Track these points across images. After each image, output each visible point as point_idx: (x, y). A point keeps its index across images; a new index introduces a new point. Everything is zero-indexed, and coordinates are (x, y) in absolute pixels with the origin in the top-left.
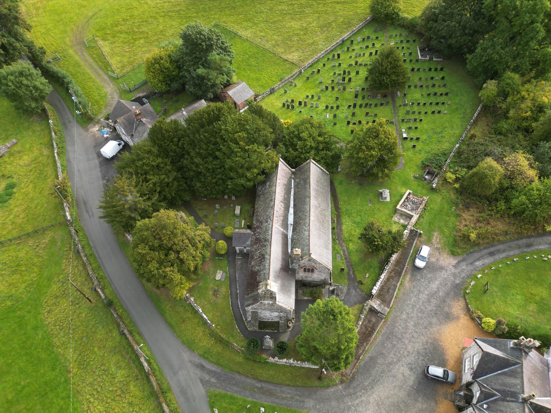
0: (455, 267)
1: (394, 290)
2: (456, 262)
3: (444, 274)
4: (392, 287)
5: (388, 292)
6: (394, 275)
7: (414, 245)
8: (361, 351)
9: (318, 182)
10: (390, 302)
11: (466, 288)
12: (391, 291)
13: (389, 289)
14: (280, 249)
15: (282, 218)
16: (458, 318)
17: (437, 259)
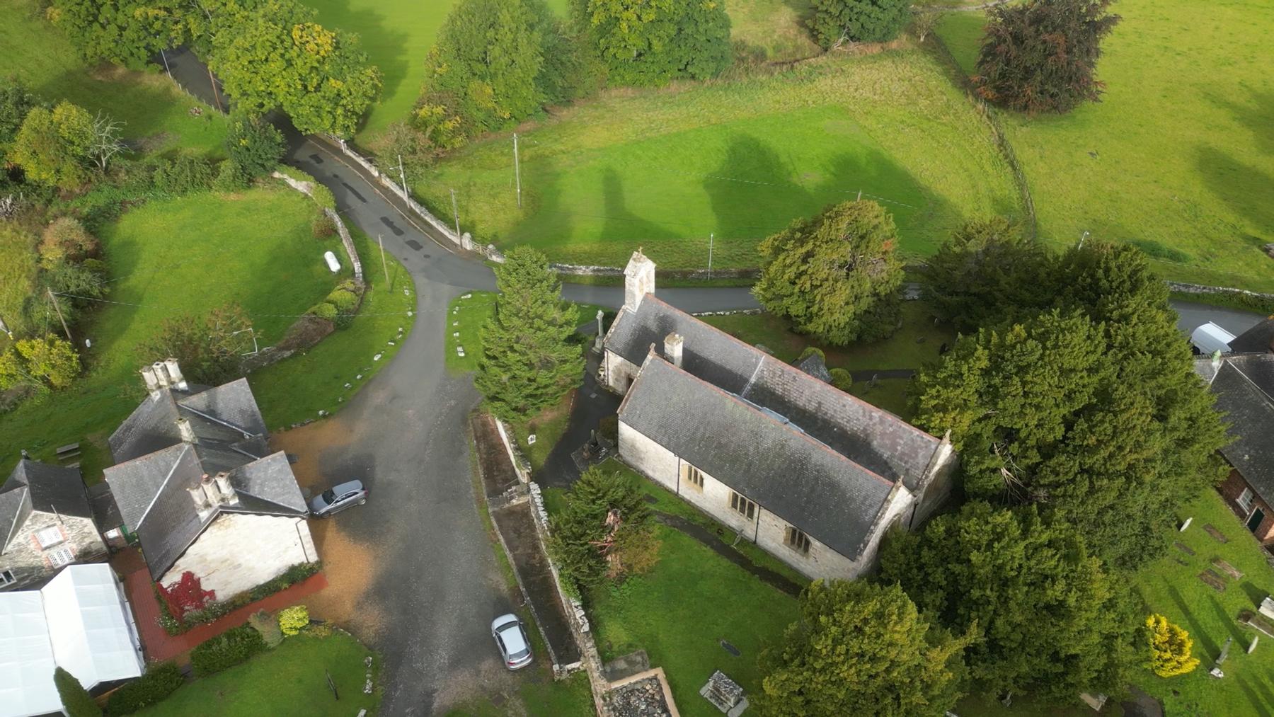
0: (429, 694)
1: (508, 542)
2: (435, 705)
3: (443, 656)
4: (517, 543)
5: (516, 531)
6: (534, 561)
7: (550, 649)
8: (482, 446)
9: (833, 486)
10: (498, 521)
11: (376, 667)
12: (512, 535)
13: (519, 537)
14: (712, 358)
15: (779, 391)
16: (359, 606)
17: (478, 673)
